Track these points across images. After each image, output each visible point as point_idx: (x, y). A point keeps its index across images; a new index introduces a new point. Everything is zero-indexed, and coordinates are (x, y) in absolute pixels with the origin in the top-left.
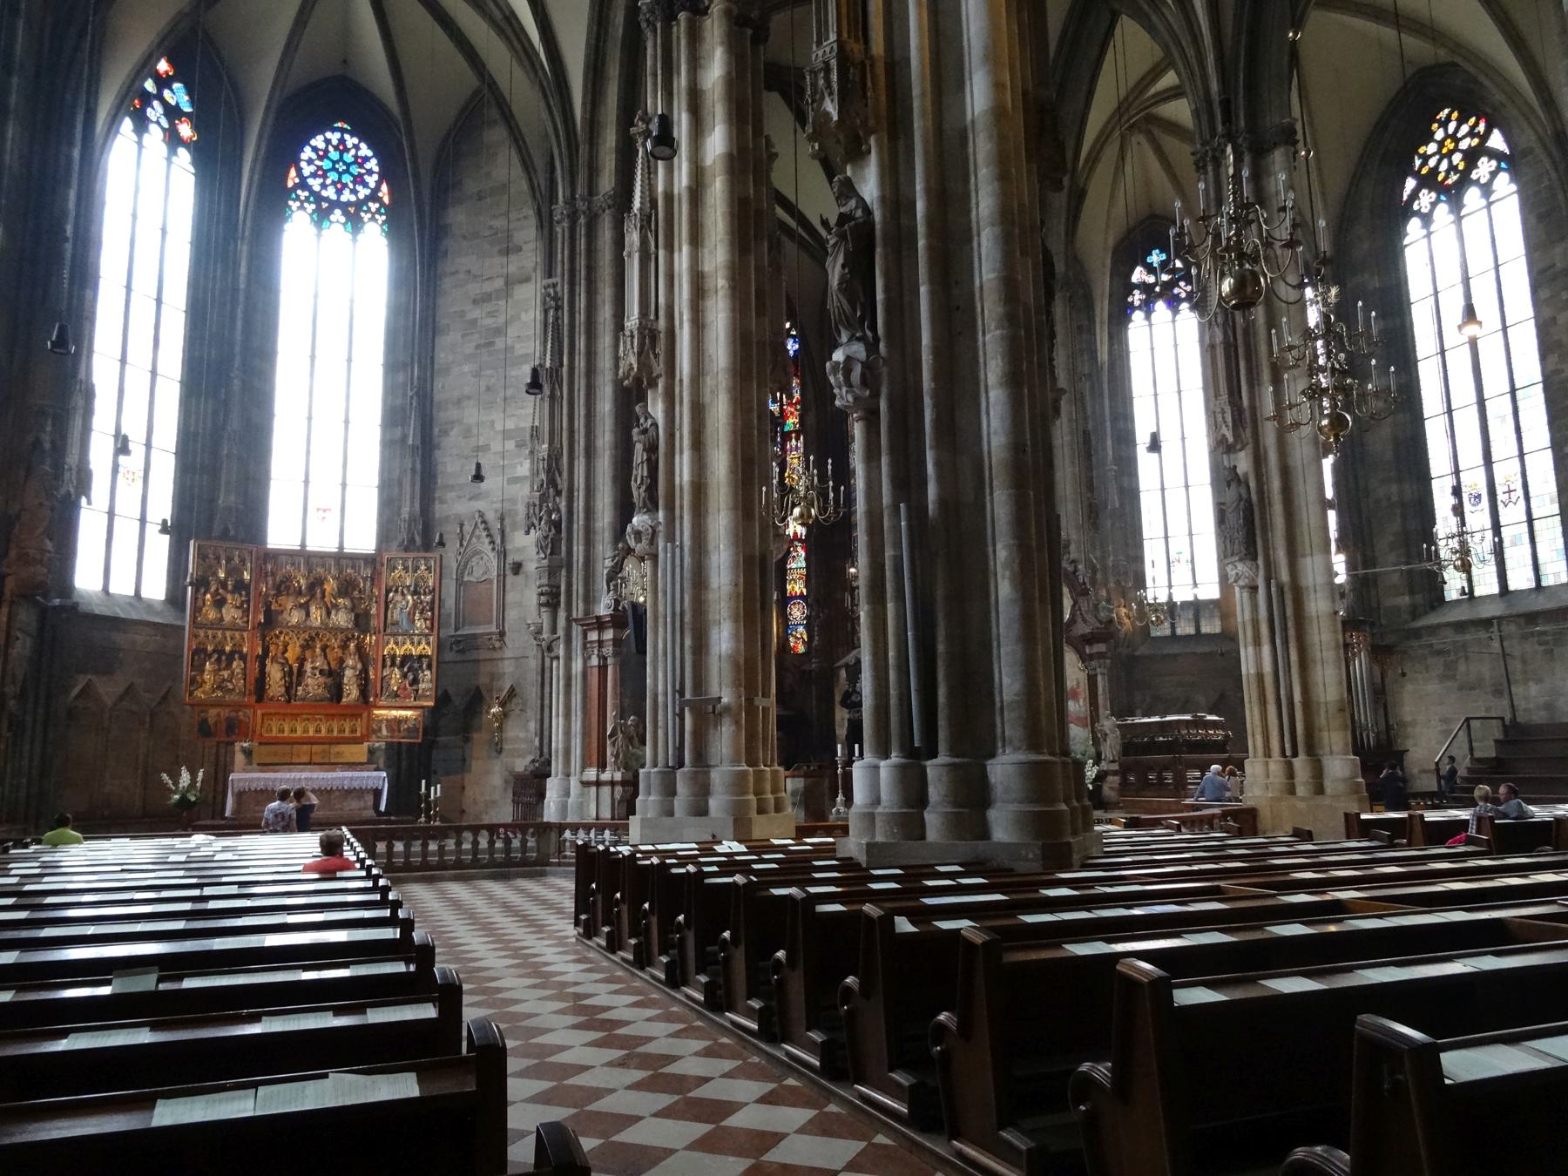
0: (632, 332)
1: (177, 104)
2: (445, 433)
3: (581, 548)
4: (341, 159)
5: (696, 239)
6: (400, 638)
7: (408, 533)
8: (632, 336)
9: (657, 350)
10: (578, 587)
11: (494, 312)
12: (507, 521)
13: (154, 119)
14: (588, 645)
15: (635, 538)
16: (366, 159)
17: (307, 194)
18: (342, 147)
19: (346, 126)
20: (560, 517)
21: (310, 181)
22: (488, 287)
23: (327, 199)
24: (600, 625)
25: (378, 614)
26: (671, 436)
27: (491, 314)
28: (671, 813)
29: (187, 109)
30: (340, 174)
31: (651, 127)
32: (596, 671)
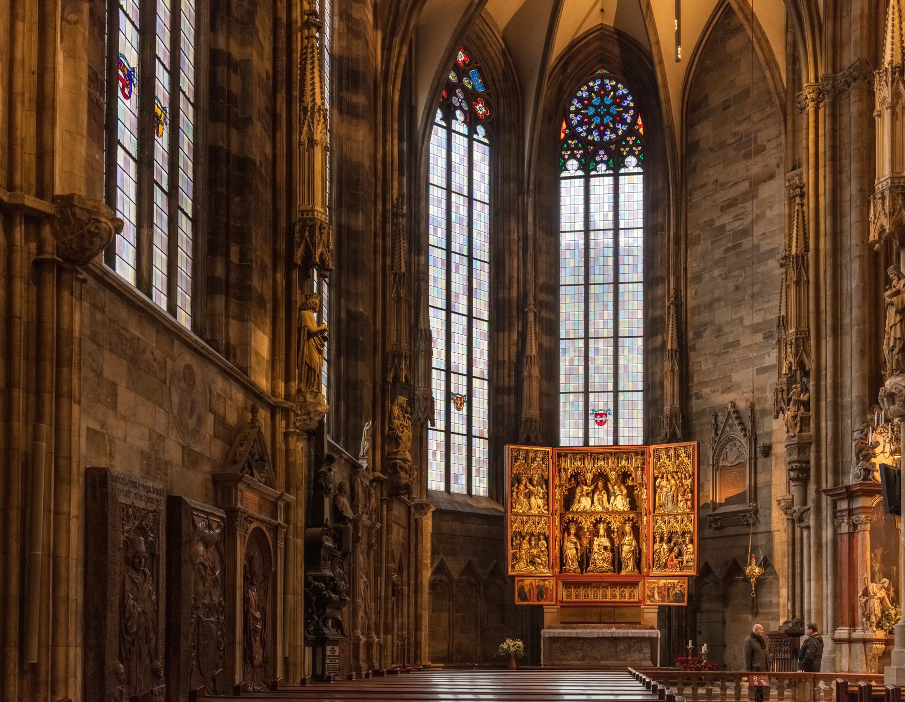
3: (829, 423)
6: (666, 518)
11: (741, 214)
13: (458, 104)
14: (838, 514)
16: (624, 97)
17: (575, 141)
18: (603, 92)
21: (579, 130)
22: (733, 193)
23: (592, 143)
25: (648, 499)
27: (737, 218)
29: (481, 90)
30: (602, 117)
32: (846, 538)
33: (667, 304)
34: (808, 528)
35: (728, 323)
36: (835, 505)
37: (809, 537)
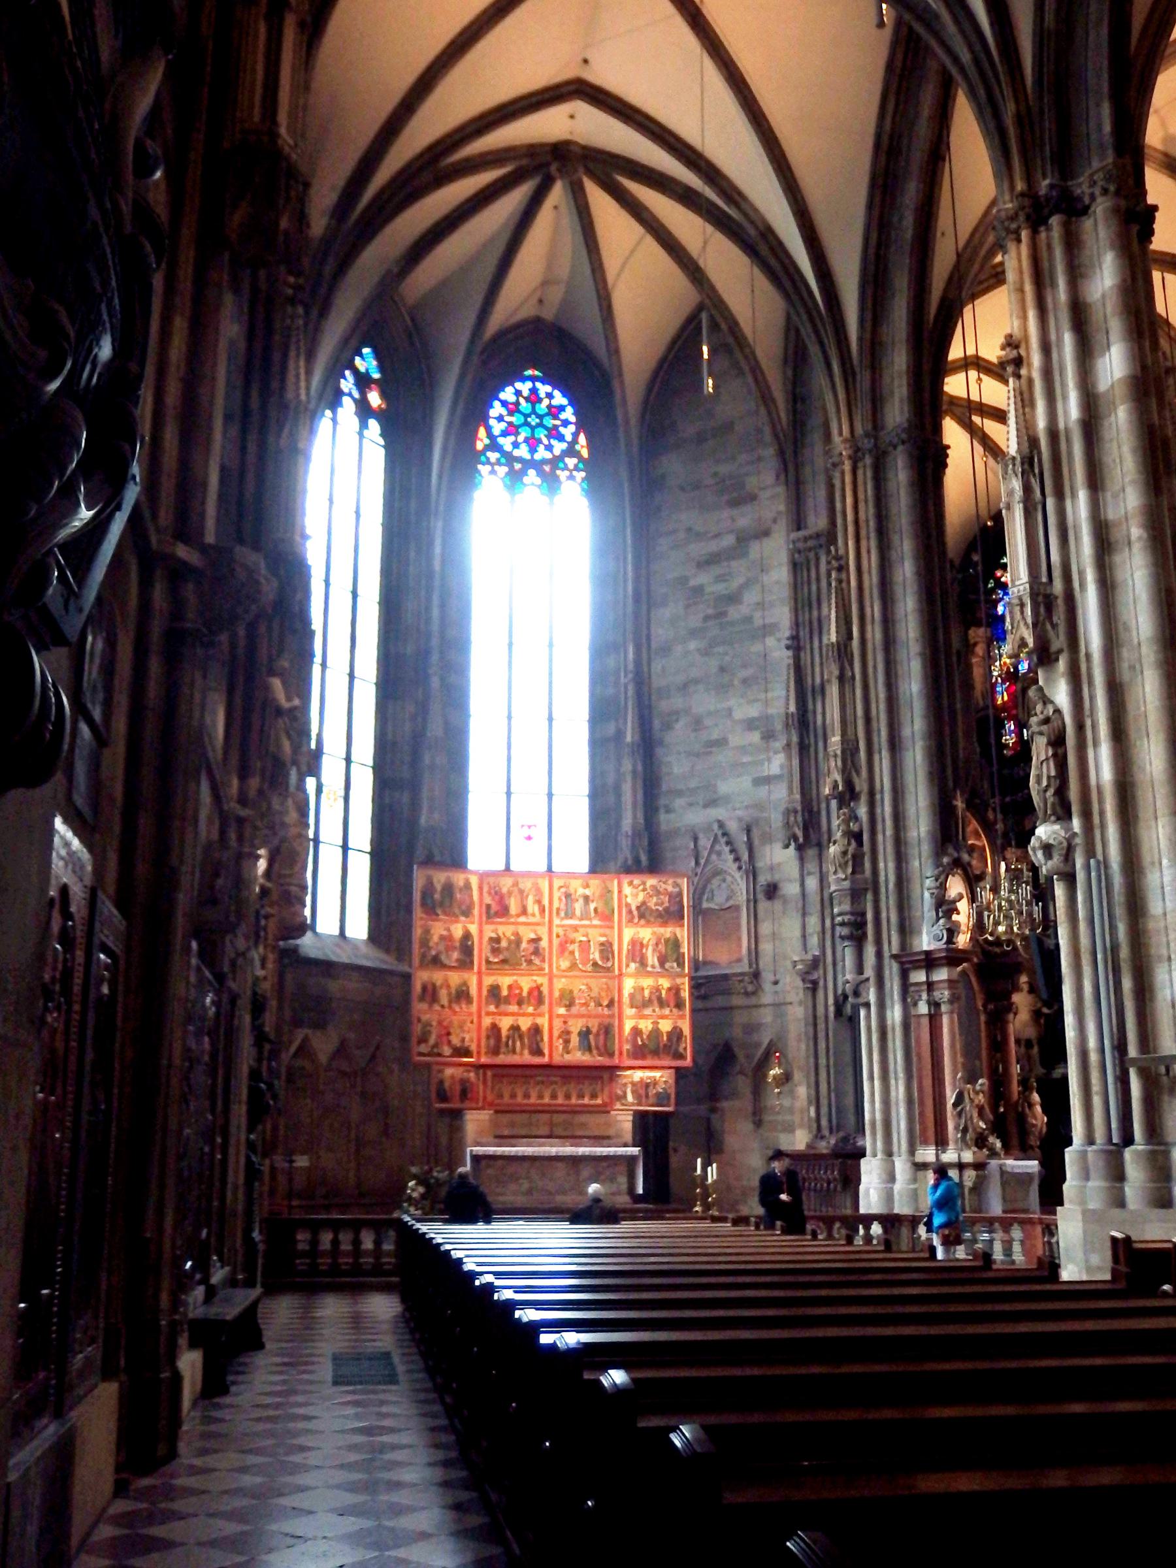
0: (1020, 598)
1: (367, 370)
2: (667, 726)
4: (534, 412)
5: (1095, 482)
7: (632, 852)
8: (1022, 605)
9: (1055, 619)
10: (890, 914)
11: (724, 575)
12: (756, 833)
15: (1044, 854)
16: (562, 408)
18: (534, 398)
19: (537, 373)
20: (861, 826)
21: (501, 440)
23: (520, 460)
24: (929, 961)
26: (1080, 727)
27: (720, 578)
28: (1121, 1203)
29: (376, 375)
31: (1023, 352)
32: (925, 1022)
33: (623, 680)
34: (867, 1005)
35: (710, 714)
36: (904, 975)
37: (868, 1016)
